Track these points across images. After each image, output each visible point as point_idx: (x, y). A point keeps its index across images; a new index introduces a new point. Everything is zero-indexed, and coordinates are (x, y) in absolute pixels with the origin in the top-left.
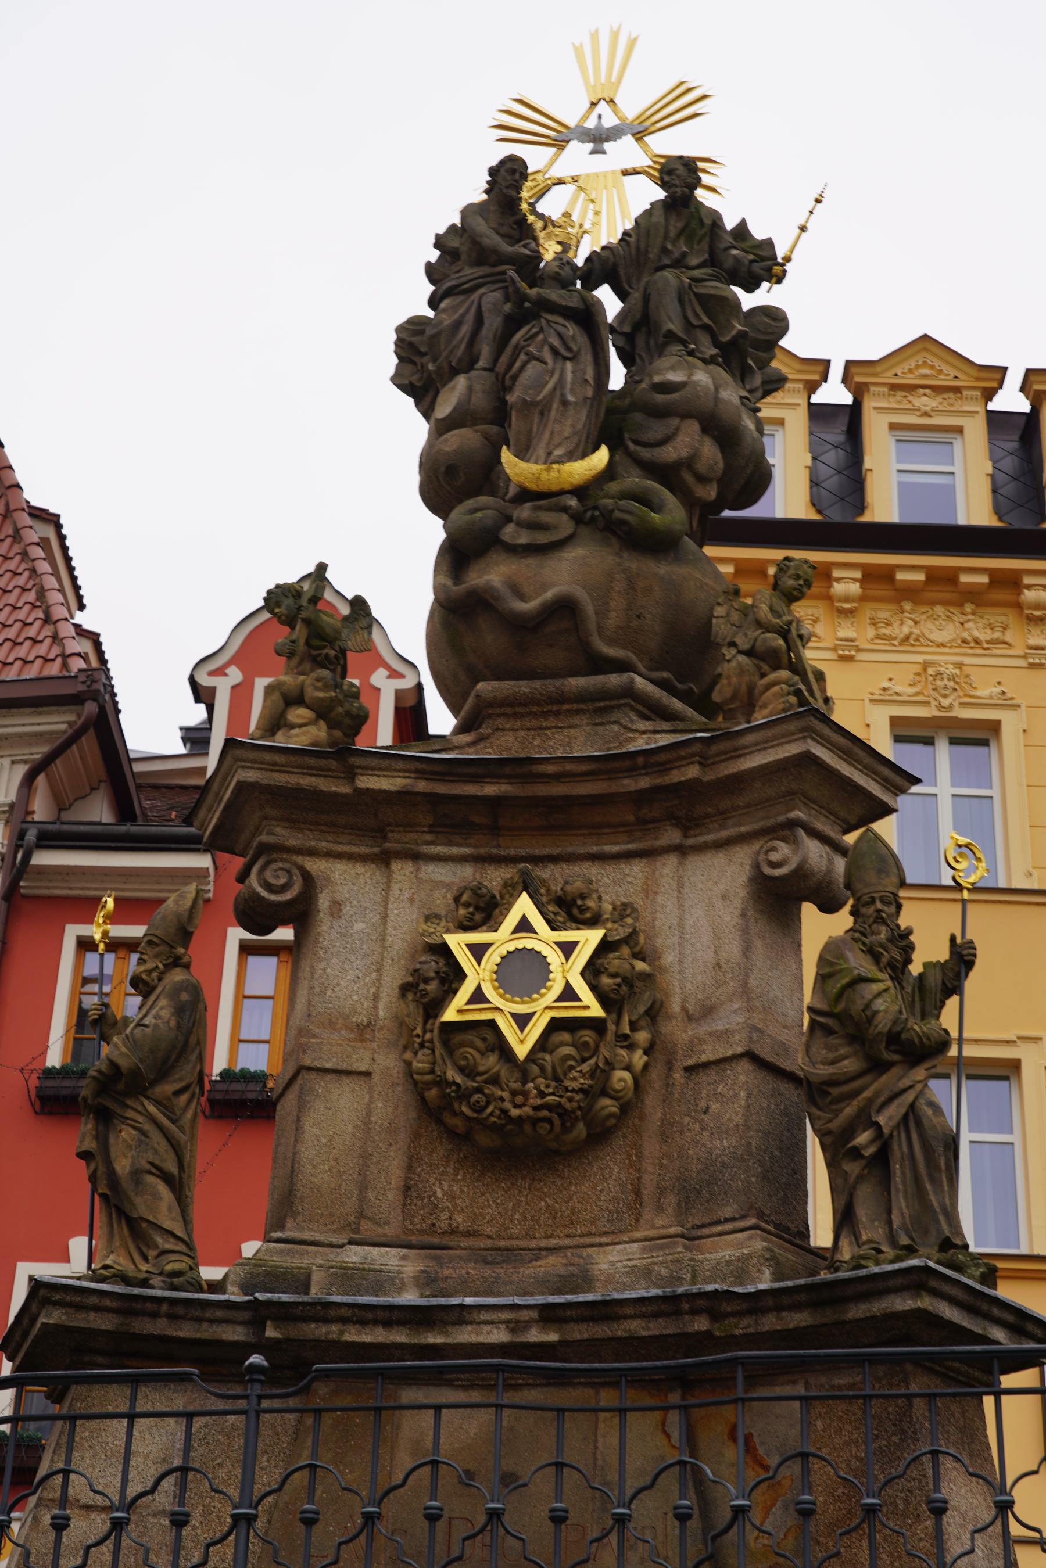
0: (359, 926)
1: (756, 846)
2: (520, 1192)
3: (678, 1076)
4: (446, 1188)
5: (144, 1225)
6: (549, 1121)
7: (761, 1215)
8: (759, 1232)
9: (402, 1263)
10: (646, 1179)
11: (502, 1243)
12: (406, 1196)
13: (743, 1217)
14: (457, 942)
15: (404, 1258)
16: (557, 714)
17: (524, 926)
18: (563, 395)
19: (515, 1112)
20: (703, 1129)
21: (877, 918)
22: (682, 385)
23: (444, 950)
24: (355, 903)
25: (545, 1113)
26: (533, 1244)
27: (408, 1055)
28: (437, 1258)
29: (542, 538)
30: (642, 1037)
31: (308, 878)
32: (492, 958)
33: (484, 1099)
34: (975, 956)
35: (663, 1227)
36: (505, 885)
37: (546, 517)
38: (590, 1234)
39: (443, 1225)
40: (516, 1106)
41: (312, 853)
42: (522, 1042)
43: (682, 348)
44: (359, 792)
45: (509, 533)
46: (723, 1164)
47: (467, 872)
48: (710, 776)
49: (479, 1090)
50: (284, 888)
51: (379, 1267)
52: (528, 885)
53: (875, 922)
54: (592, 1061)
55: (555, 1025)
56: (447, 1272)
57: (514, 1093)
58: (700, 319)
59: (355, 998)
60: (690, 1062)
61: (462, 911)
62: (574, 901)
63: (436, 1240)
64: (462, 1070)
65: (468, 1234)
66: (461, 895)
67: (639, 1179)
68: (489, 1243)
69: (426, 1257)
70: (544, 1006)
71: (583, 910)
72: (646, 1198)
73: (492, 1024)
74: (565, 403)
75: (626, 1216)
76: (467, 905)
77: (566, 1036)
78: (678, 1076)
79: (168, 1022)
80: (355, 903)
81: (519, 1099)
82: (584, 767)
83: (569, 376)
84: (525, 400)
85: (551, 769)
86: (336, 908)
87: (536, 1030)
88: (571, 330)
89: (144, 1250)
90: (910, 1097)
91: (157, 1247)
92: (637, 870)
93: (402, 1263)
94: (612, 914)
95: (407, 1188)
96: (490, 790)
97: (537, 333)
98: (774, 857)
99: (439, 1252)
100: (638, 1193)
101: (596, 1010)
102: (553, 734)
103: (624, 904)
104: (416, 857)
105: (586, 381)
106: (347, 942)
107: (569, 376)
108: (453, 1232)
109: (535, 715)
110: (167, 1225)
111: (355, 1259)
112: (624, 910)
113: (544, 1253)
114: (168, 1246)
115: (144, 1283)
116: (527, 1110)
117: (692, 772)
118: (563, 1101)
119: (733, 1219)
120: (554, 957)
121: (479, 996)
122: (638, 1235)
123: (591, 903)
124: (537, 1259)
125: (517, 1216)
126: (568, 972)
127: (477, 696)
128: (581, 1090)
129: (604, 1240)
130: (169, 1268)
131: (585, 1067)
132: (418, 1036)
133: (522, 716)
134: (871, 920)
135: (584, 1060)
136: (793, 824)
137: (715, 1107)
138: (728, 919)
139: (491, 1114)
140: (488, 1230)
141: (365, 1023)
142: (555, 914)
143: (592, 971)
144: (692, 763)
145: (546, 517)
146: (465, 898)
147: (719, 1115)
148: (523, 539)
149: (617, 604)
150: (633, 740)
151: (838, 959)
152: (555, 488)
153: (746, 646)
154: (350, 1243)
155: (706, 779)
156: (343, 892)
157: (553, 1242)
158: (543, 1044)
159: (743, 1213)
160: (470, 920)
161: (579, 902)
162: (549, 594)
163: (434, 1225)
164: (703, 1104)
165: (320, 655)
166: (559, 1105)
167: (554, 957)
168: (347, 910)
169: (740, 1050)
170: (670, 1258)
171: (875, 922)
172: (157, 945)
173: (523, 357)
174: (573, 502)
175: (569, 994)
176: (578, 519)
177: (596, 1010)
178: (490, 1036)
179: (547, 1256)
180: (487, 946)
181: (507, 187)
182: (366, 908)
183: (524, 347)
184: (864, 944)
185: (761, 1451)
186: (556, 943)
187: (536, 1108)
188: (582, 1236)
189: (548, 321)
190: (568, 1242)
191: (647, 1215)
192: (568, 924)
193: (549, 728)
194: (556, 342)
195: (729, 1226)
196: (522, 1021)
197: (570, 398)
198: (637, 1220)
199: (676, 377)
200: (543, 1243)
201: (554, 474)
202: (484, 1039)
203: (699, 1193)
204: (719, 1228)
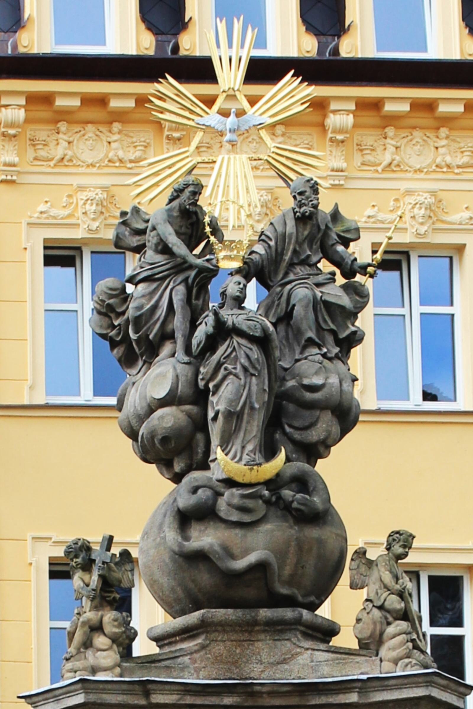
18: (250, 402)
22: (323, 386)
29: (247, 518)
37: (250, 503)
43: (318, 352)
58: (329, 326)
74: (252, 408)
82: (285, 689)
83: (254, 388)
84: (230, 411)
88: (255, 353)
96: (228, 701)
97: (231, 353)
105: (265, 390)
107: (254, 388)
117: (353, 698)
144: (354, 692)
145: (250, 503)
148: (235, 516)
149: (291, 560)
152: (253, 481)
153: (379, 603)
162: (252, 558)
165: (109, 597)
173: (222, 372)
174: (266, 493)
176: (267, 502)
181: (190, 204)
183: (224, 363)
189: (238, 343)
194: (247, 364)
197: (257, 406)
199: (318, 380)
201: (254, 472)
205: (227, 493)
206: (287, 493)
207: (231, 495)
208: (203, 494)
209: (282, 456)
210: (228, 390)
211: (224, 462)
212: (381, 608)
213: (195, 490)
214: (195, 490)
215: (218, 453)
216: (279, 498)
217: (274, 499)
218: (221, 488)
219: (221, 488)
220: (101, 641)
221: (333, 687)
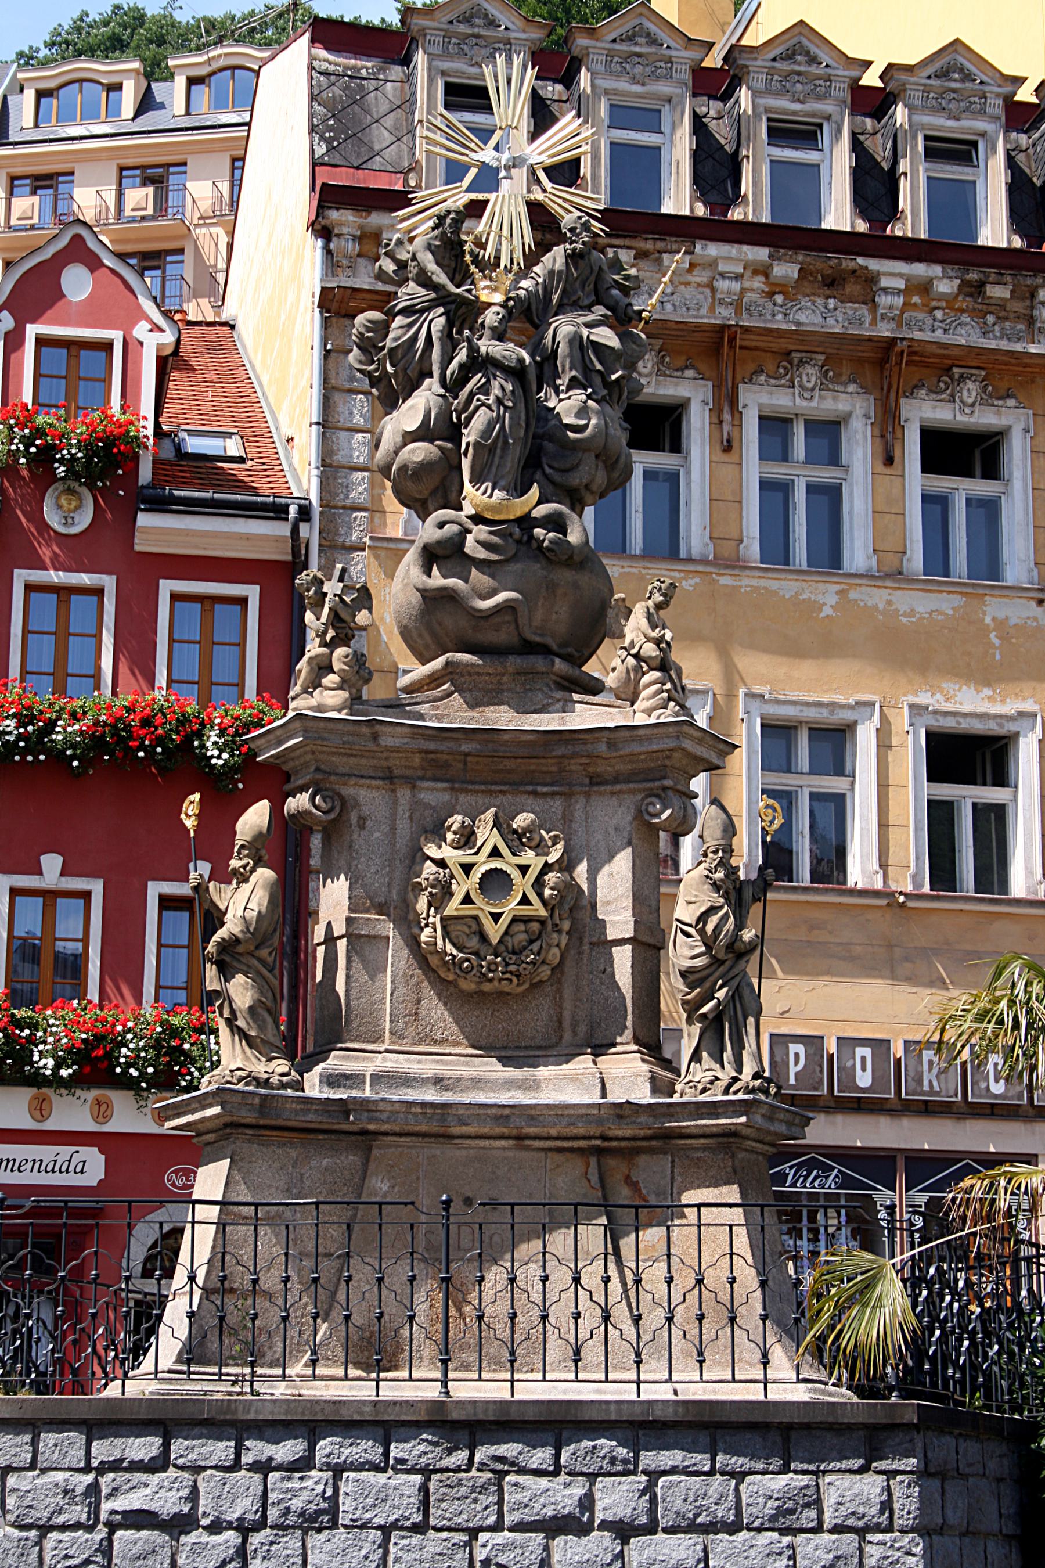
0: (377, 834)
3: (586, 947)
17: (495, 853)
25: (508, 976)
30: (566, 925)
40: (490, 971)
45: (470, 545)
55: (515, 920)
64: (454, 945)
70: (511, 906)
73: (476, 918)
77: (522, 927)
78: (586, 947)
86: (362, 821)
87: (504, 922)
100: (560, 1023)
101: (543, 913)
120: (515, 874)
126: (522, 885)
129: (540, 1053)
136: (665, 789)
156: (366, 811)
164: (602, 968)
167: (515, 874)
176: (519, 542)
177: (543, 913)
178: (475, 927)
180: (472, 865)
185: (644, 1191)
202: (470, 927)
205: (475, 529)
206: (538, 532)
207: (480, 531)
208: (451, 529)
209: (534, 492)
210: (481, 419)
211: (474, 496)
212: (636, 656)
213: (441, 525)
214: (441, 525)
215: (468, 487)
216: (531, 537)
217: (525, 538)
218: (469, 525)
219: (469, 525)
220: (331, 680)
221: (581, 736)
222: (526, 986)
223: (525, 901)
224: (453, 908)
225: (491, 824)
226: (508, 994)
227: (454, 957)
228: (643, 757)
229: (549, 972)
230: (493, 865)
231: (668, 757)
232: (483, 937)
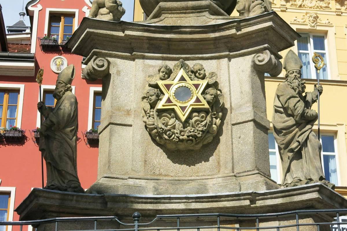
1: (253, 55)
2: (181, 162)
4: (158, 161)
5: (63, 172)
6: (191, 140)
7: (258, 170)
8: (259, 175)
9: (146, 184)
10: (221, 159)
11: (177, 178)
12: (145, 164)
13: (253, 170)
14: (161, 83)
15: (146, 183)
16: (185, 13)
17: (182, 79)
19: (181, 137)
20: (239, 143)
21: (295, 78)
23: (156, 86)
24: (124, 71)
25: (191, 138)
26: (187, 178)
27: (145, 119)
28: (156, 183)
31: (109, 63)
32: (173, 89)
33: (171, 133)
34: (322, 90)
35: (227, 173)
36: (175, 66)
38: (204, 175)
39: (157, 173)
41: (111, 56)
42: (184, 115)
44: (125, 35)
46: (246, 154)
47: (160, 63)
48: (239, 33)
49: (169, 130)
50: (103, 66)
51: (140, 186)
52: (183, 66)
53: (294, 79)
54: (206, 121)
55: (193, 111)
56: (161, 187)
57: (181, 132)
59: (126, 101)
60: (234, 122)
61: (161, 74)
62: (197, 72)
63: (156, 177)
65: (165, 176)
66: (161, 69)
67: (219, 158)
68: (172, 178)
69: (153, 182)
70: (190, 104)
71: (200, 74)
72: (221, 165)
73: (173, 110)
75: (215, 170)
76: (163, 72)
79: (68, 108)
80: (124, 71)
81: (182, 133)
85: (188, 30)
86: (118, 73)
89: (63, 180)
90: (307, 133)
91: (68, 179)
92: (214, 61)
93: (146, 184)
94: (209, 75)
95: (145, 161)
98: (260, 59)
99: (157, 181)
100: (219, 163)
101: (207, 106)
102: (184, 19)
103: (213, 73)
104: (144, 58)
106: (122, 84)
108: (160, 175)
109: (178, 13)
110: (70, 172)
111: (131, 183)
112: (212, 74)
113: (190, 181)
114: (71, 179)
115: (66, 190)
116: (185, 137)
117: (233, 31)
118: (196, 134)
119: (250, 171)
121: (169, 101)
122: (220, 176)
123: (202, 72)
124: (189, 183)
125: (180, 170)
126: (198, 93)
127: (160, 7)
128: (202, 131)
129: (209, 177)
130: (73, 185)
131: (203, 123)
132: (148, 113)
133: (174, 13)
134: (293, 78)
135: (202, 121)
137: (242, 136)
138: (244, 78)
139: (174, 138)
140: (172, 175)
141: (129, 109)
142: (191, 75)
143: (203, 93)
144: (233, 29)
146: (162, 70)
147: (244, 139)
150: (210, 21)
151: (284, 90)
154: (129, 178)
155: (238, 33)
156: (120, 68)
157: (193, 178)
158: (190, 117)
159: (253, 169)
160: (164, 77)
161: (199, 72)
163: (154, 173)
164: (239, 136)
166: (195, 135)
167: (193, 88)
168: (122, 73)
169: (250, 119)
170: (232, 182)
171: (294, 79)
172: (62, 84)
175: (198, 100)
179: (191, 182)
182: (128, 73)
184: (291, 86)
186: (193, 84)
187: (188, 136)
188: (201, 176)
190: (198, 178)
191: (222, 169)
192: (195, 79)
193: (183, 17)
195: (250, 173)
196: (183, 109)
198: (219, 171)
200: (190, 178)
203: (239, 163)
204: (246, 174)
222: (200, 145)
223: (198, 100)
224: (160, 105)
225: (180, 67)
226: (192, 150)
227: (163, 129)
228: (254, 36)
229: (212, 138)
230: (181, 85)
231: (267, 34)
232: (177, 118)
